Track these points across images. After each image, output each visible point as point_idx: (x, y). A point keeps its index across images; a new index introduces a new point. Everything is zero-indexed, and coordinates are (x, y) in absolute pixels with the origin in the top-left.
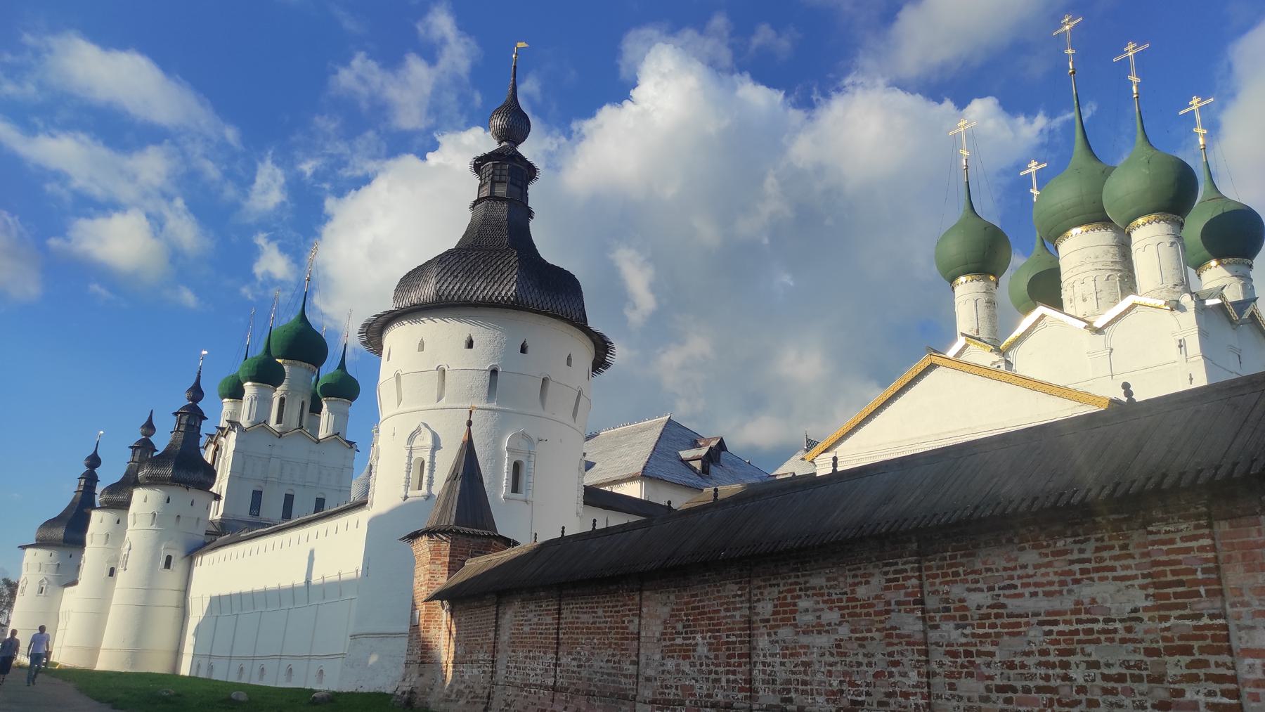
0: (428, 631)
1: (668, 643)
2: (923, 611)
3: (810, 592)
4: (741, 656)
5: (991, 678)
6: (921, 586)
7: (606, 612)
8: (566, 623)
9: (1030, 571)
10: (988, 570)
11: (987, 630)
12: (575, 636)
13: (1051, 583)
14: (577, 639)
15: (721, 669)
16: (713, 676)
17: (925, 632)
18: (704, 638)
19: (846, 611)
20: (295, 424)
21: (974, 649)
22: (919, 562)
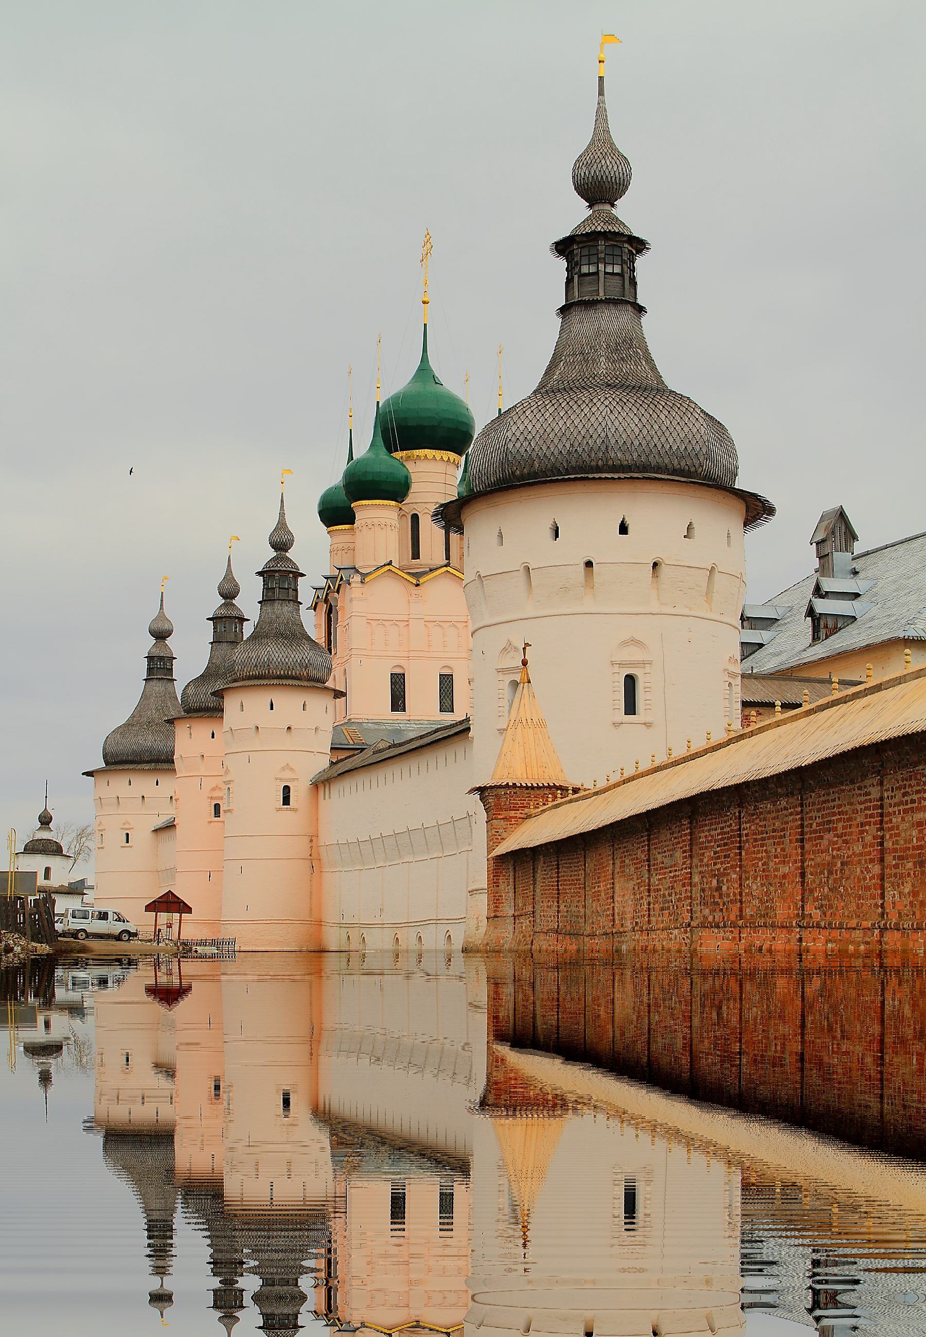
0: (498, 886)
2: (649, 866)
6: (649, 850)
11: (661, 877)
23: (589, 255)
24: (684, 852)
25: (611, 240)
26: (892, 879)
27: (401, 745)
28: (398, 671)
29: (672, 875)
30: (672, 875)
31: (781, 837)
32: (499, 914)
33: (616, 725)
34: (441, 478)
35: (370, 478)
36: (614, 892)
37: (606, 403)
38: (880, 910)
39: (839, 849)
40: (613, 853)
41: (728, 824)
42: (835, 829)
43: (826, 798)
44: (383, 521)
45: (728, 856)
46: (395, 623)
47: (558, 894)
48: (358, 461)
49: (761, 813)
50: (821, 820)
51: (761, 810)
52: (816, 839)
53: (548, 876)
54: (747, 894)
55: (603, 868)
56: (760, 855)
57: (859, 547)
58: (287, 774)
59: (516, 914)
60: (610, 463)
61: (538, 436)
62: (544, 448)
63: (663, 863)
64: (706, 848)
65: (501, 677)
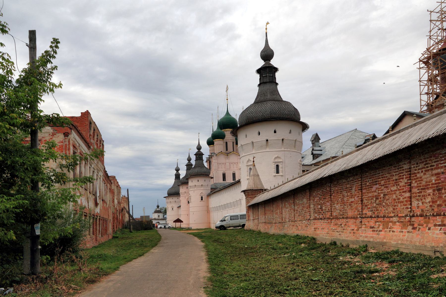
2: (294, 204)
17: (294, 207)
26: (417, 198)
28: (224, 173)
29: (302, 206)
30: (302, 206)
31: (350, 190)
32: (249, 219)
38: (409, 210)
39: (382, 190)
41: (325, 189)
42: (380, 183)
43: (374, 173)
45: (326, 198)
46: (223, 163)
49: (340, 183)
50: (371, 181)
51: (340, 183)
52: (368, 188)
54: (334, 209)
56: (340, 197)
63: (299, 203)
64: (316, 197)
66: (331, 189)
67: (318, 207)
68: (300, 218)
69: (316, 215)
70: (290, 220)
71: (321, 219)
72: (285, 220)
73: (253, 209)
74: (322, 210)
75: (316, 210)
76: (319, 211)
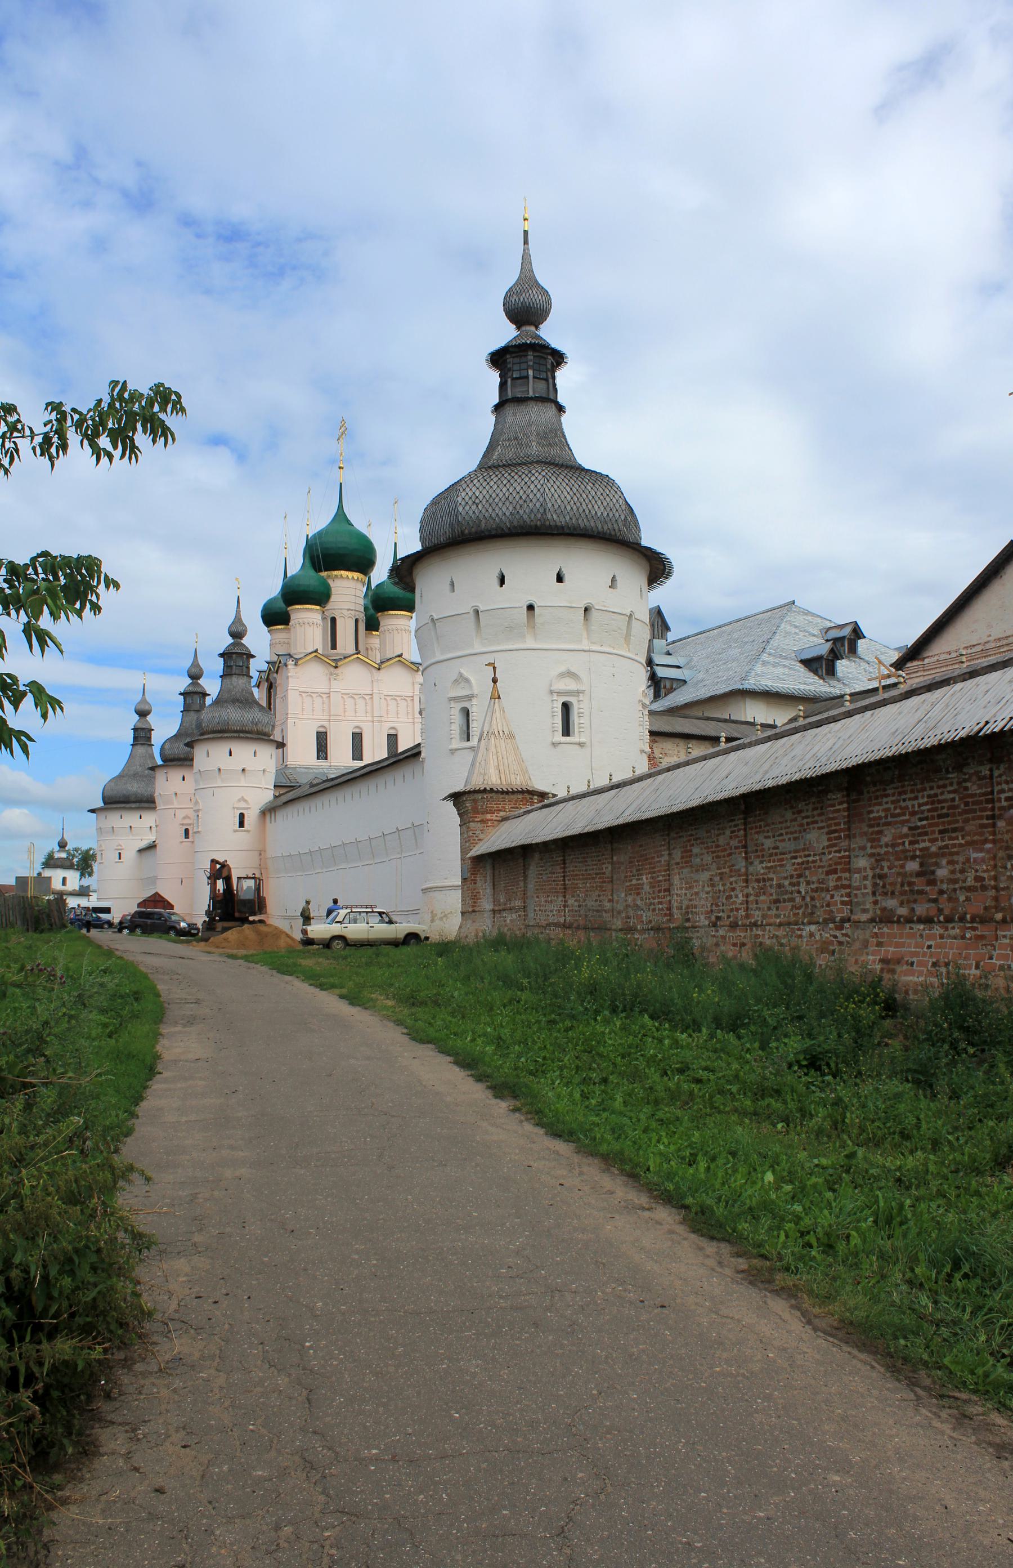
0: (475, 883)
1: (628, 884)
2: (746, 853)
3: (698, 842)
4: (665, 891)
5: (771, 895)
6: (745, 836)
7: (593, 861)
8: (569, 872)
9: (788, 824)
10: (773, 823)
11: (772, 864)
12: (576, 882)
13: (795, 832)
14: (577, 884)
15: (656, 901)
16: (652, 907)
17: (747, 868)
18: (647, 879)
19: (715, 855)
20: (351, 649)
21: (766, 877)
22: (745, 819)
23: (520, 363)
24: (829, 833)
25: (538, 351)
27: (333, 779)
29: (799, 860)
32: (477, 909)
33: (554, 745)
34: (353, 592)
35: (301, 589)
36: (671, 885)
37: (543, 473)
40: (669, 843)
44: (311, 621)
46: (320, 695)
47: (565, 888)
48: (293, 577)
53: (547, 872)
55: (647, 859)
57: (671, 636)
58: (242, 805)
59: (497, 908)
60: (547, 523)
61: (484, 500)
62: (490, 510)
65: (453, 704)
66: (996, 789)
67: (903, 866)
68: (786, 912)
69: (891, 903)
70: (718, 918)
71: (928, 921)
72: (688, 920)
73: (494, 868)
74: (932, 882)
75: (889, 880)
76: (910, 884)
